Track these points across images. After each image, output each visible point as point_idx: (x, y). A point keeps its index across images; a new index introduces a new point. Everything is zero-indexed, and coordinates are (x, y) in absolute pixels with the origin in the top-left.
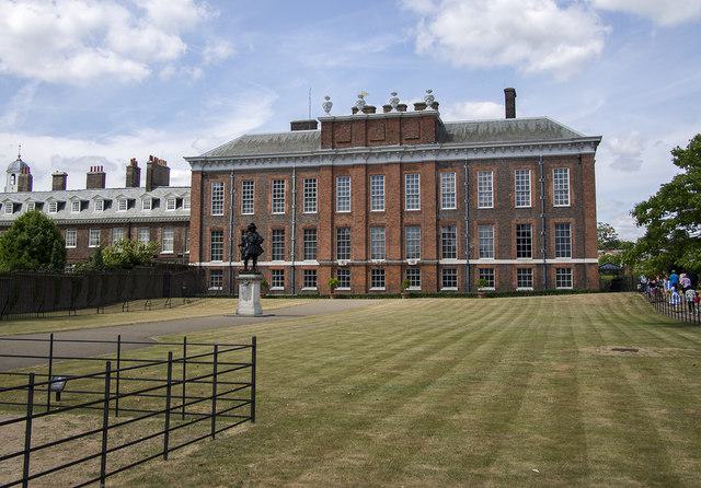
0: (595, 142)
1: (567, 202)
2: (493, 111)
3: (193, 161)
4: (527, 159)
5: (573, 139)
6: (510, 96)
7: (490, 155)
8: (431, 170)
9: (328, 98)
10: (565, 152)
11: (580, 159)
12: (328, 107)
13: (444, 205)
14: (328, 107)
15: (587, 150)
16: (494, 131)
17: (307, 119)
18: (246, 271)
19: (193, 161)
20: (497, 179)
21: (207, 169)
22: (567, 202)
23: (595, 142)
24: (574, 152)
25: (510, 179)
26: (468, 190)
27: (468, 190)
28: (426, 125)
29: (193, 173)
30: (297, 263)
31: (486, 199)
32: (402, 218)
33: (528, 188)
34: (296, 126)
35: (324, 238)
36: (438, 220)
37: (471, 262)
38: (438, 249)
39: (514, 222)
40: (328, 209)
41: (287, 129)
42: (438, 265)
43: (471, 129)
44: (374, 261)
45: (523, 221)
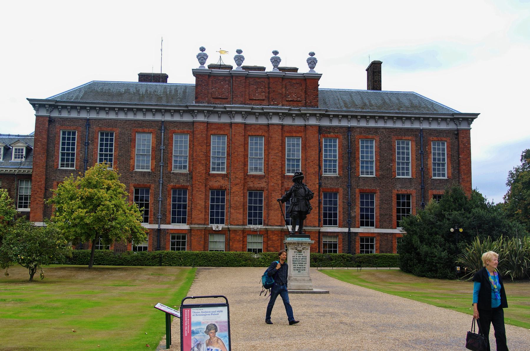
0: (470, 118)
1: (443, 175)
2: (360, 83)
3: (36, 104)
4: (408, 130)
5: (453, 114)
6: (374, 71)
7: (372, 124)
8: (313, 137)
9: (203, 49)
10: (443, 126)
11: (457, 134)
12: (202, 58)
13: (325, 171)
14: (202, 58)
15: (463, 126)
16: (370, 102)
17: (157, 71)
18: (294, 234)
19: (36, 104)
20: (380, 148)
21: (55, 114)
22: (443, 175)
23: (470, 118)
24: (452, 126)
25: (391, 148)
26: (350, 156)
27: (350, 156)
28: (296, 88)
29: (38, 118)
30: (163, 227)
31: (368, 170)
32: (282, 183)
33: (408, 159)
34: (143, 77)
35: (199, 201)
36: (320, 186)
37: (353, 230)
38: (319, 216)
39: (395, 192)
40: (201, 168)
41: (136, 79)
42: (319, 232)
43: (346, 98)
44: (252, 226)
45: (404, 191)
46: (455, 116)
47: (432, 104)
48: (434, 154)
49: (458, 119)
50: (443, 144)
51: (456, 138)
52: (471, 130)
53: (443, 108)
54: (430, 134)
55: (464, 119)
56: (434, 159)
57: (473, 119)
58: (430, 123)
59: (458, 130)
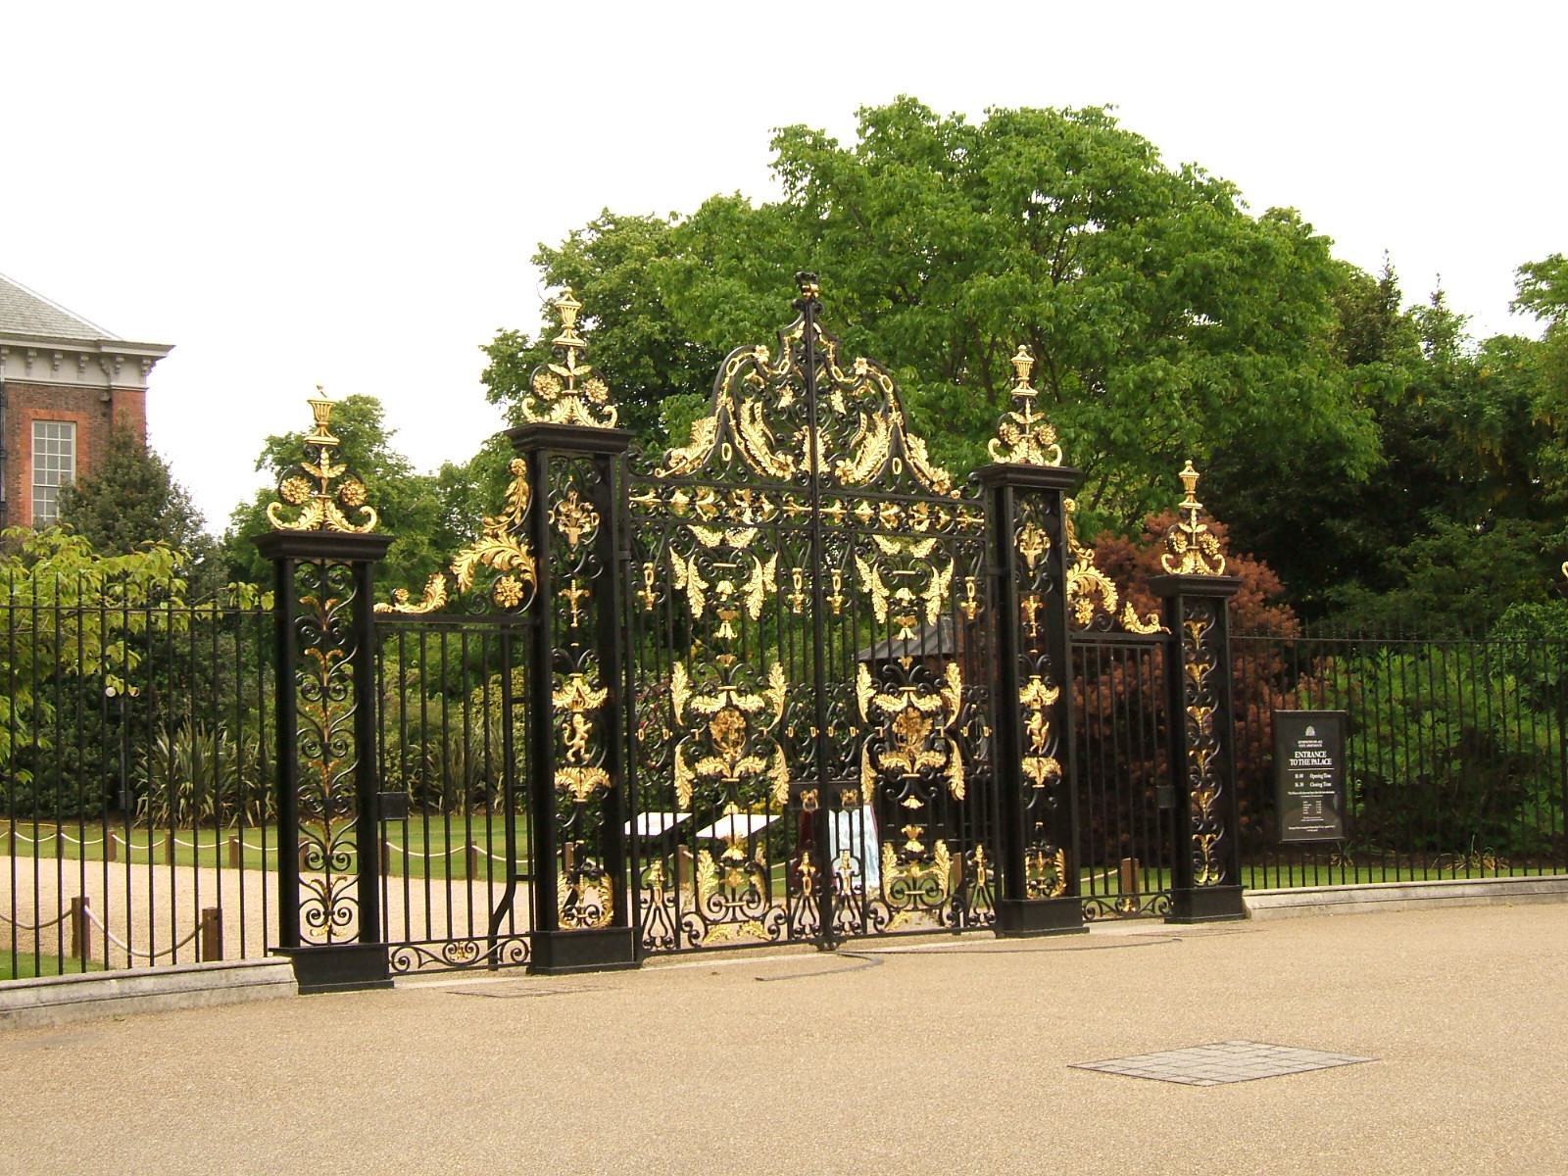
0: (142, 359)
5: (97, 344)
10: (67, 376)
11: (109, 403)
15: (125, 379)
23: (142, 359)
24: (93, 379)
46: (105, 349)
47: (34, 302)
48: (40, 461)
49: (112, 357)
50: (66, 434)
51: (104, 415)
52: (148, 392)
53: (67, 318)
54: (30, 400)
55: (129, 358)
56: (39, 476)
57: (154, 359)
58: (28, 365)
59: (109, 390)
